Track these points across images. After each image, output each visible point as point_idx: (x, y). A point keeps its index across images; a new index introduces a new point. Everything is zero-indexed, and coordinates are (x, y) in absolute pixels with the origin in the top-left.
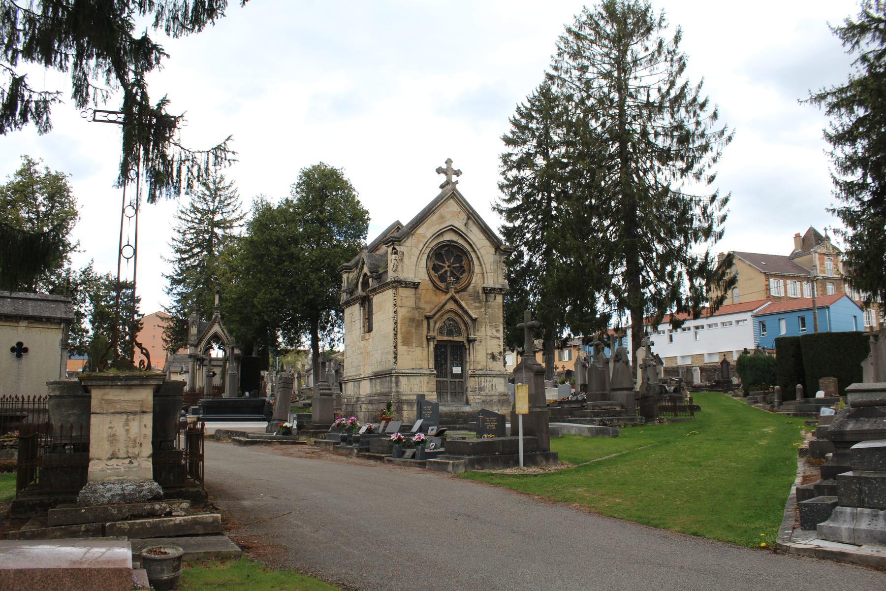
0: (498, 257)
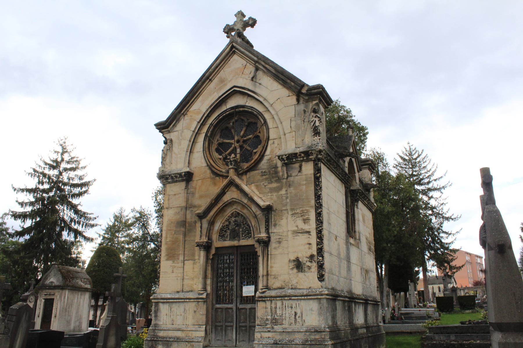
0: (302, 107)
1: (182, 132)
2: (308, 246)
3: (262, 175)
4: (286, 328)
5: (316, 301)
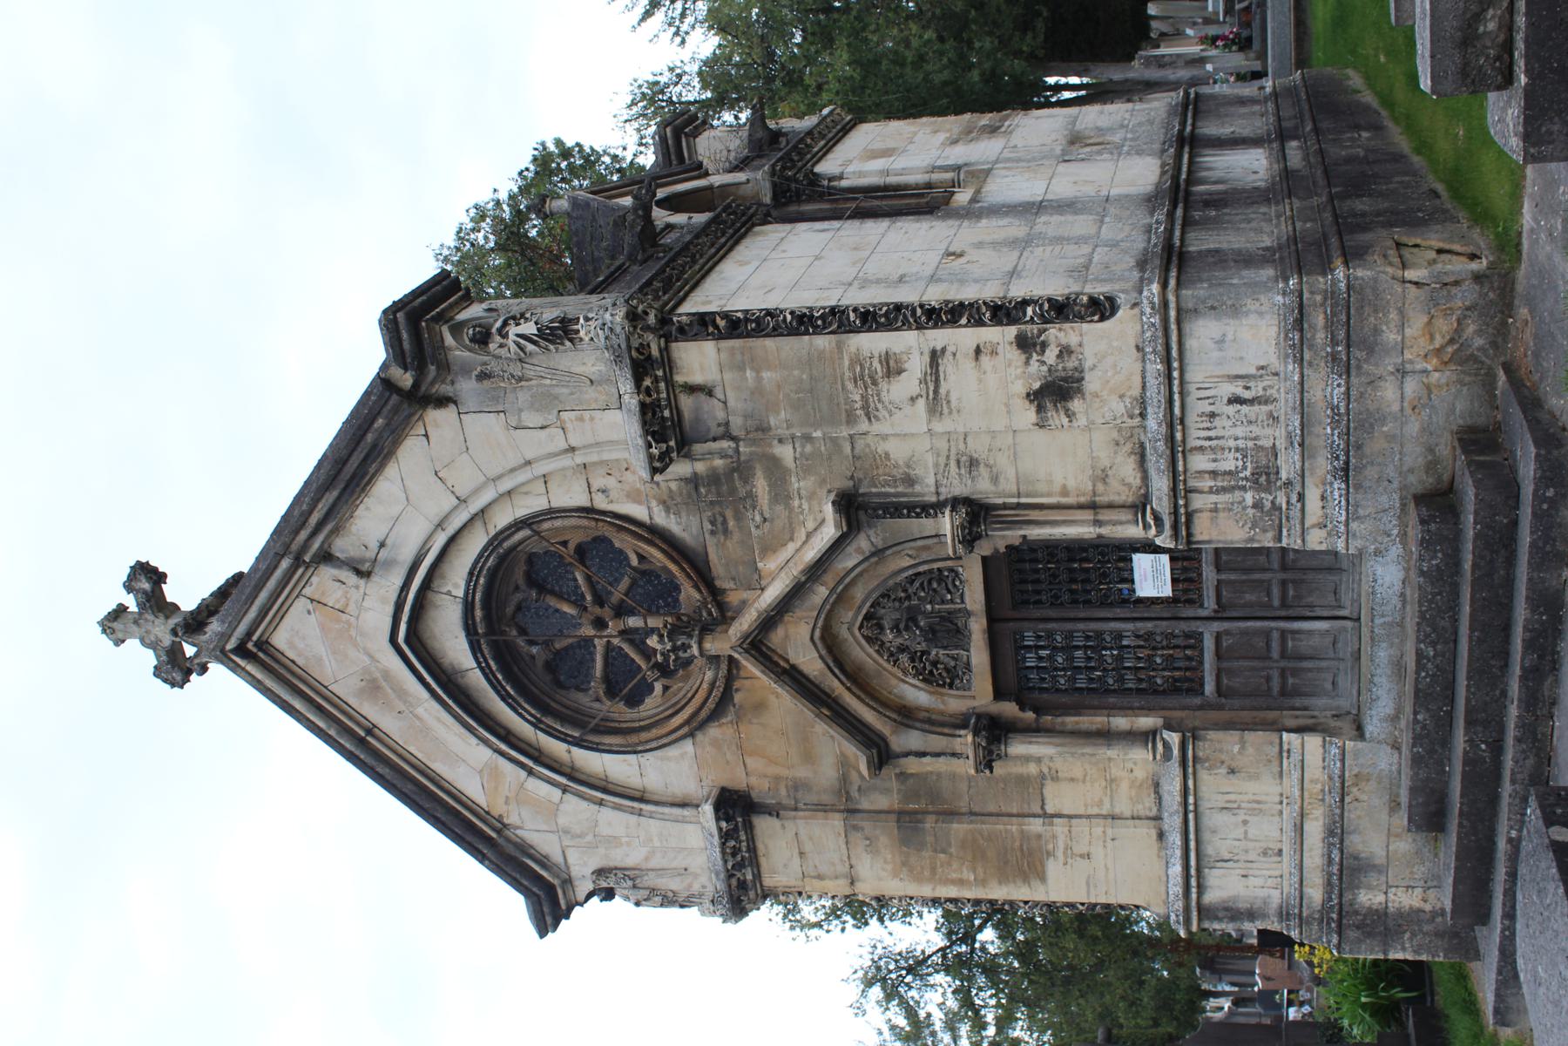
0: (466, 387)
1: (566, 832)
2: (984, 359)
3: (726, 531)
4: (1289, 436)
5: (1187, 327)
